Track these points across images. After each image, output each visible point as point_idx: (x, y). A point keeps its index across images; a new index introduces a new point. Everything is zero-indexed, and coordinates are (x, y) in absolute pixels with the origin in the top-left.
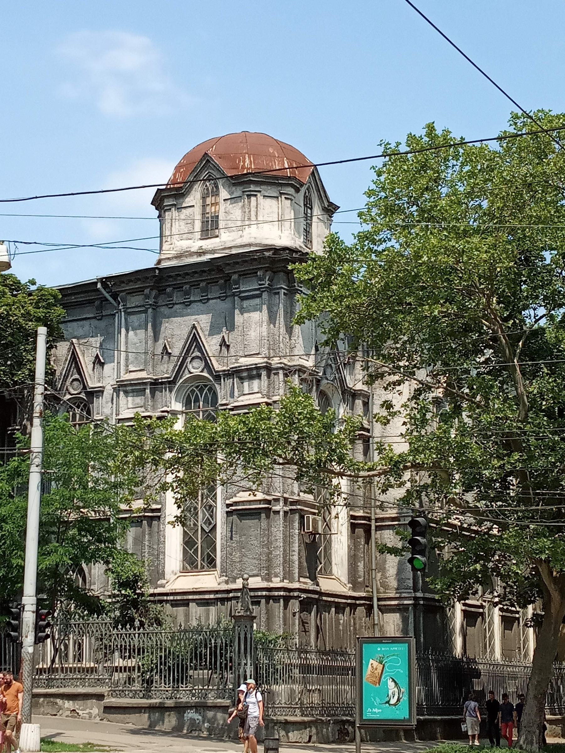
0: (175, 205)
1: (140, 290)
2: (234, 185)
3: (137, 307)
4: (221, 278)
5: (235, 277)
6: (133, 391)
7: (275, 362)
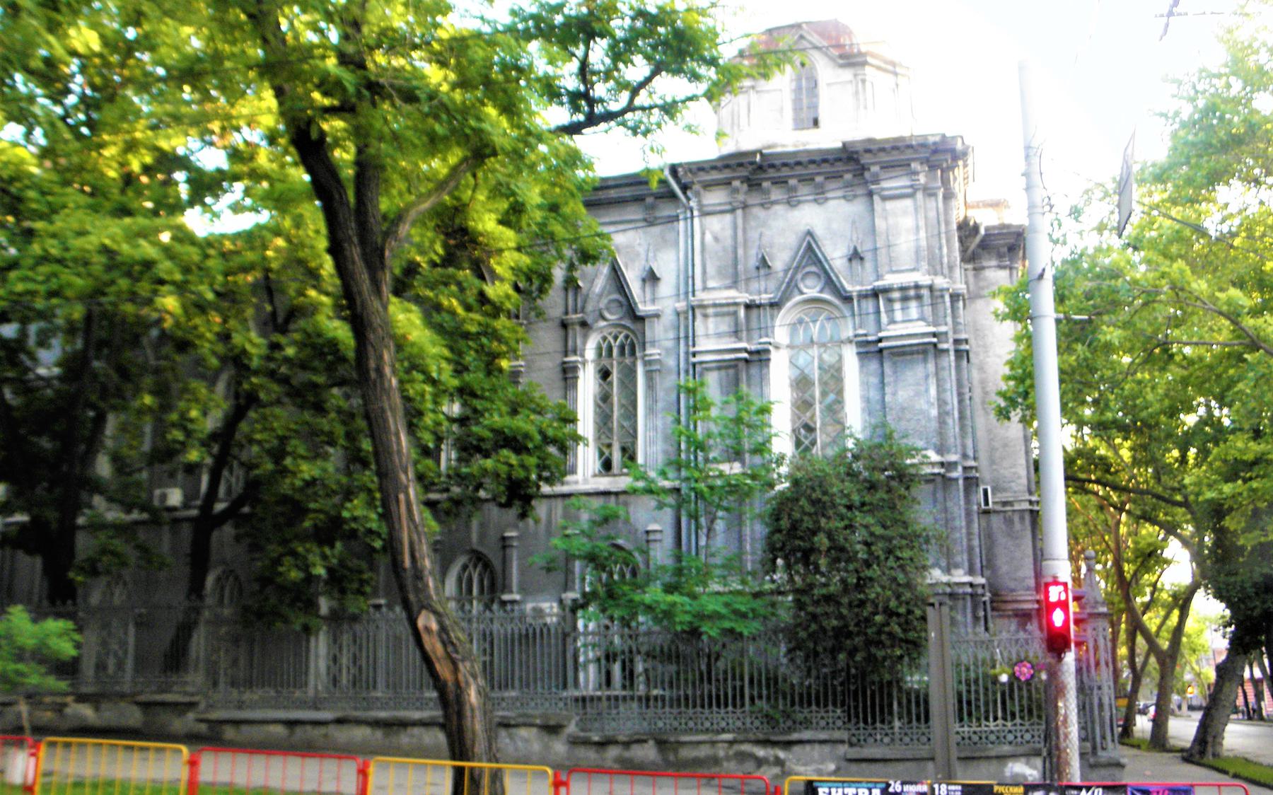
0: (753, 87)
1: (727, 183)
2: (842, 66)
3: (720, 204)
4: (848, 171)
5: (875, 169)
6: (716, 315)
7: (940, 282)
